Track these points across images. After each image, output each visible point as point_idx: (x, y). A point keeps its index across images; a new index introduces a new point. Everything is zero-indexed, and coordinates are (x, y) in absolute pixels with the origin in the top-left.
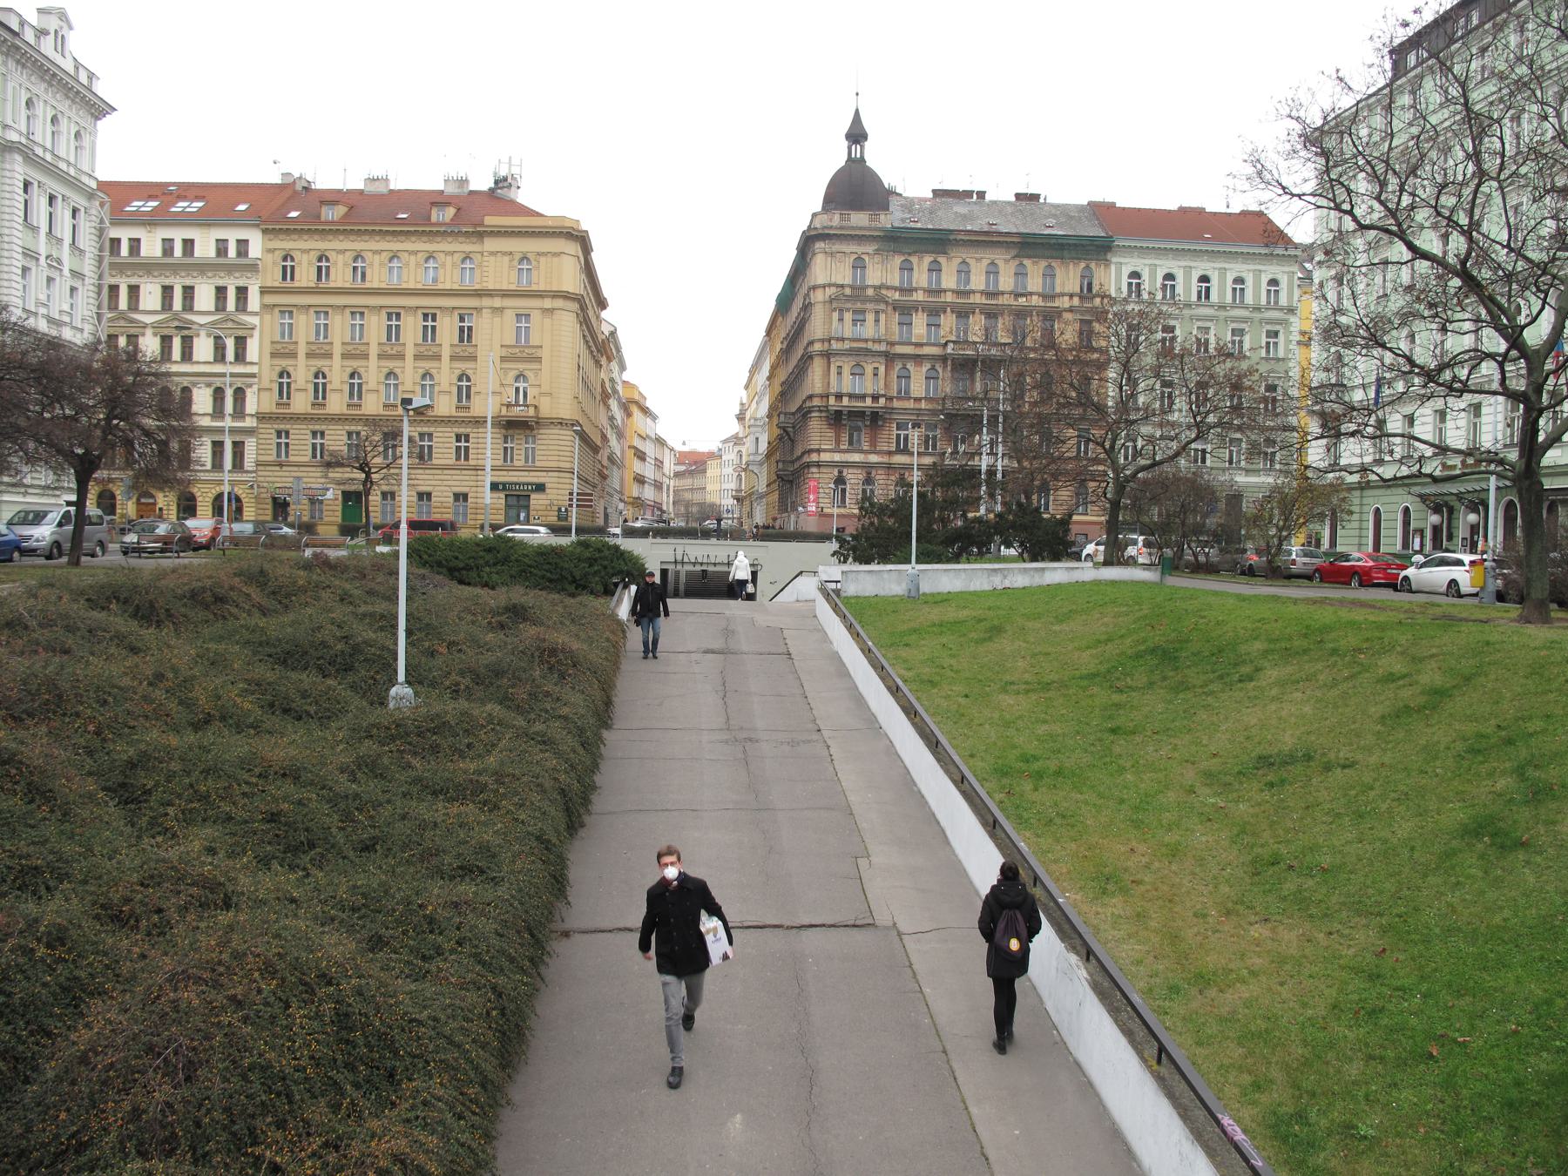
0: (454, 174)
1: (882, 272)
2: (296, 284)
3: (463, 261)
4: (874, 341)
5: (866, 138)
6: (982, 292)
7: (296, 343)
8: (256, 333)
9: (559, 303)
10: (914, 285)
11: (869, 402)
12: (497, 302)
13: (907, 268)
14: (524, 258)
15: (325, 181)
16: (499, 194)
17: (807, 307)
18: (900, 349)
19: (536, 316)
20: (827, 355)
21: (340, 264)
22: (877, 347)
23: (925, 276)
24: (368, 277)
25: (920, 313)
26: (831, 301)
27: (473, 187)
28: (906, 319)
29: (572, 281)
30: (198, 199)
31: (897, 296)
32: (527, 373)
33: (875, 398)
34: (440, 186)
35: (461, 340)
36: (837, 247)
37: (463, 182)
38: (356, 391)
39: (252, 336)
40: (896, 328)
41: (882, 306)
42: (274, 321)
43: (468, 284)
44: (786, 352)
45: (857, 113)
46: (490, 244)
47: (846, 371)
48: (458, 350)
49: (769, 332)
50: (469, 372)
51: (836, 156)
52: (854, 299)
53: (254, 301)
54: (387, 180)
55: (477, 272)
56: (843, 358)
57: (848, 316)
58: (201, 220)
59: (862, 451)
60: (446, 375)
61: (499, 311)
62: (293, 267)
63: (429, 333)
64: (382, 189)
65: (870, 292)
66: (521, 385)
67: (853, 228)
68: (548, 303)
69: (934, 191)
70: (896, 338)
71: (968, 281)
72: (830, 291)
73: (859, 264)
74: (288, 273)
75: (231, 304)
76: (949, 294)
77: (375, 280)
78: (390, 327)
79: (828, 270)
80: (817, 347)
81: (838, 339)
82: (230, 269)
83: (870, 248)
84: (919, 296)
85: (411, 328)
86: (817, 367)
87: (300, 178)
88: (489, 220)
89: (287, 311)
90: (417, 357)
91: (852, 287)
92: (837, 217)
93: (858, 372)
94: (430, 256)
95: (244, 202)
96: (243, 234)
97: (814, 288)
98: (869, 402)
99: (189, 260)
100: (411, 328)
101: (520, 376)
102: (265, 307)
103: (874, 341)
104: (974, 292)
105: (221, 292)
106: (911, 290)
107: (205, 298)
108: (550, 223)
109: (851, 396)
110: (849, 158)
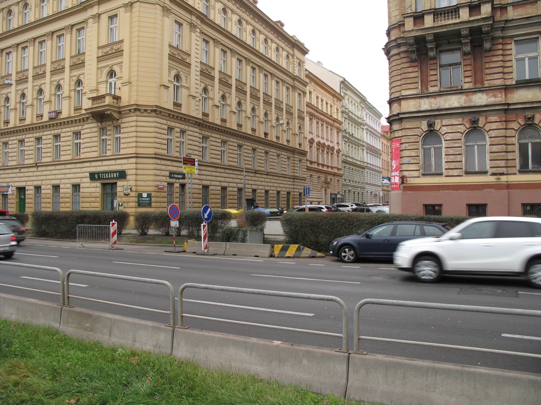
11: (464, 14)
59: (460, 91)
98: (464, 14)
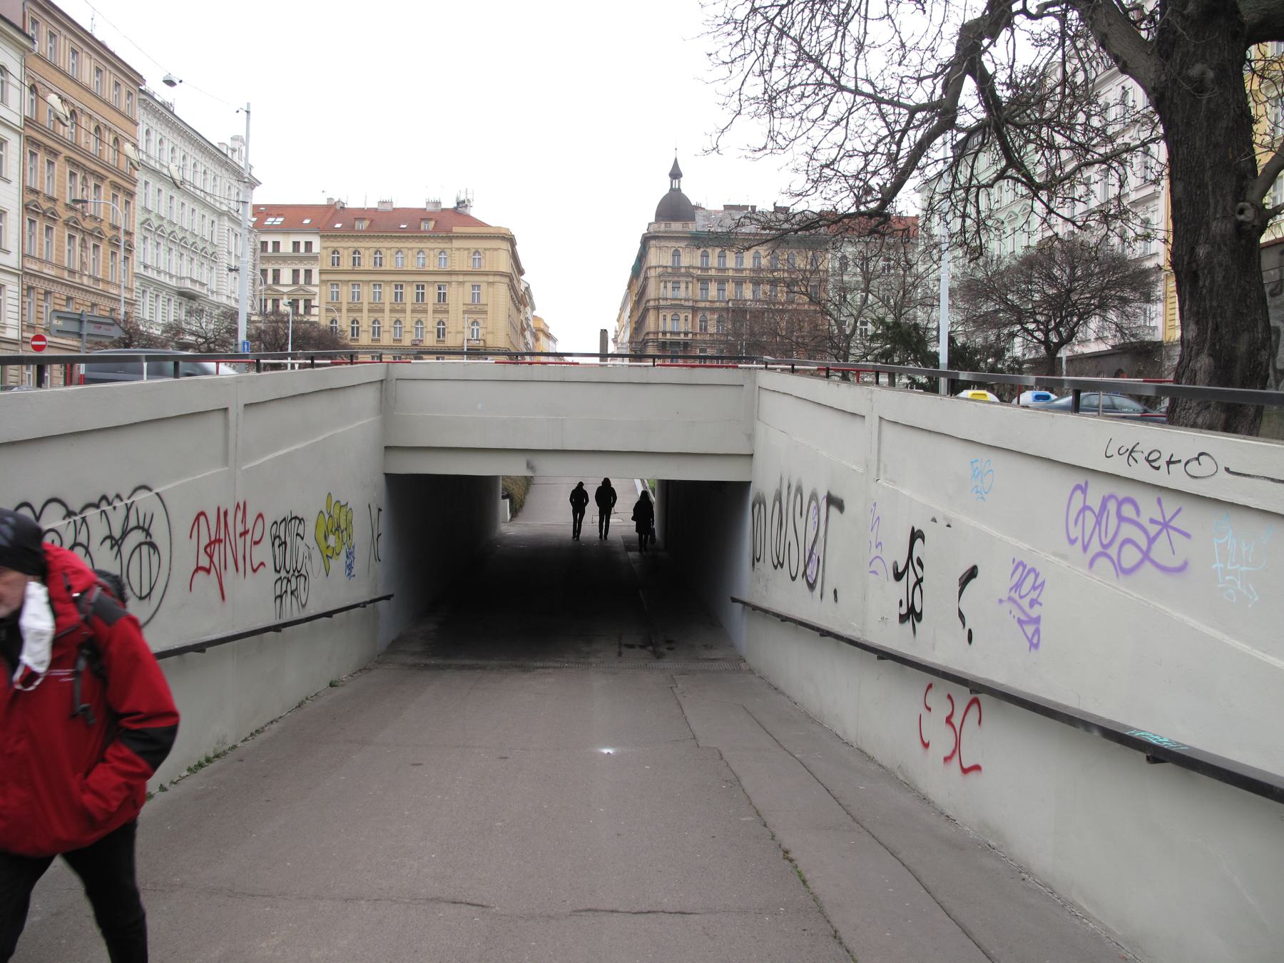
0: (432, 199)
1: (690, 258)
2: (341, 268)
3: (440, 253)
4: (685, 300)
5: (681, 176)
6: (750, 270)
7: (341, 303)
8: (317, 297)
9: (498, 278)
10: (710, 266)
11: (682, 336)
12: (461, 278)
13: (705, 255)
14: (477, 252)
15: (353, 203)
16: (460, 211)
17: (646, 278)
18: (702, 305)
19: (484, 286)
20: (657, 308)
21: (367, 255)
22: (687, 304)
23: (716, 260)
24: (383, 263)
25: (713, 282)
26: (660, 276)
27: (444, 206)
28: (704, 286)
29: (504, 265)
30: (279, 215)
31: (699, 272)
32: (479, 321)
33: (686, 334)
34: (423, 206)
35: (439, 301)
36: (663, 243)
37: (438, 203)
38: (377, 331)
39: (314, 299)
40: (699, 292)
41: (690, 279)
42: (327, 289)
43: (443, 268)
44: (637, 303)
45: (676, 160)
46: (456, 244)
47: (669, 318)
48: (437, 306)
49: (630, 286)
50: (444, 320)
51: (664, 188)
52: (673, 274)
53: (316, 278)
54: (391, 202)
55: (449, 260)
56: (667, 311)
57: (670, 285)
58: (284, 230)
60: (430, 322)
61: (462, 283)
62: (338, 258)
63: (420, 297)
64: (389, 208)
65: (683, 270)
66: (475, 327)
67: (672, 232)
68: (491, 279)
69: (724, 206)
70: (699, 298)
71: (742, 263)
72: (659, 270)
73: (676, 254)
74: (336, 261)
75: (302, 280)
76: (731, 271)
77: (388, 265)
78: (396, 293)
79: (659, 258)
80: (652, 303)
81: (663, 299)
82: (301, 259)
83: (683, 244)
84: (713, 273)
85: (409, 294)
86: (651, 316)
87: (339, 201)
88: (455, 229)
89: (335, 284)
90: (413, 311)
91: (672, 268)
92: (663, 226)
93: (675, 318)
94: (421, 251)
95: (307, 218)
96: (309, 238)
97: (650, 268)
98: (682, 336)
99: (276, 254)
100: (409, 294)
101: (475, 322)
102: (322, 282)
103: (685, 300)
104: (745, 269)
105: (296, 273)
106: (707, 269)
107: (286, 276)
108: (492, 231)
109: (672, 333)
110: (671, 189)
